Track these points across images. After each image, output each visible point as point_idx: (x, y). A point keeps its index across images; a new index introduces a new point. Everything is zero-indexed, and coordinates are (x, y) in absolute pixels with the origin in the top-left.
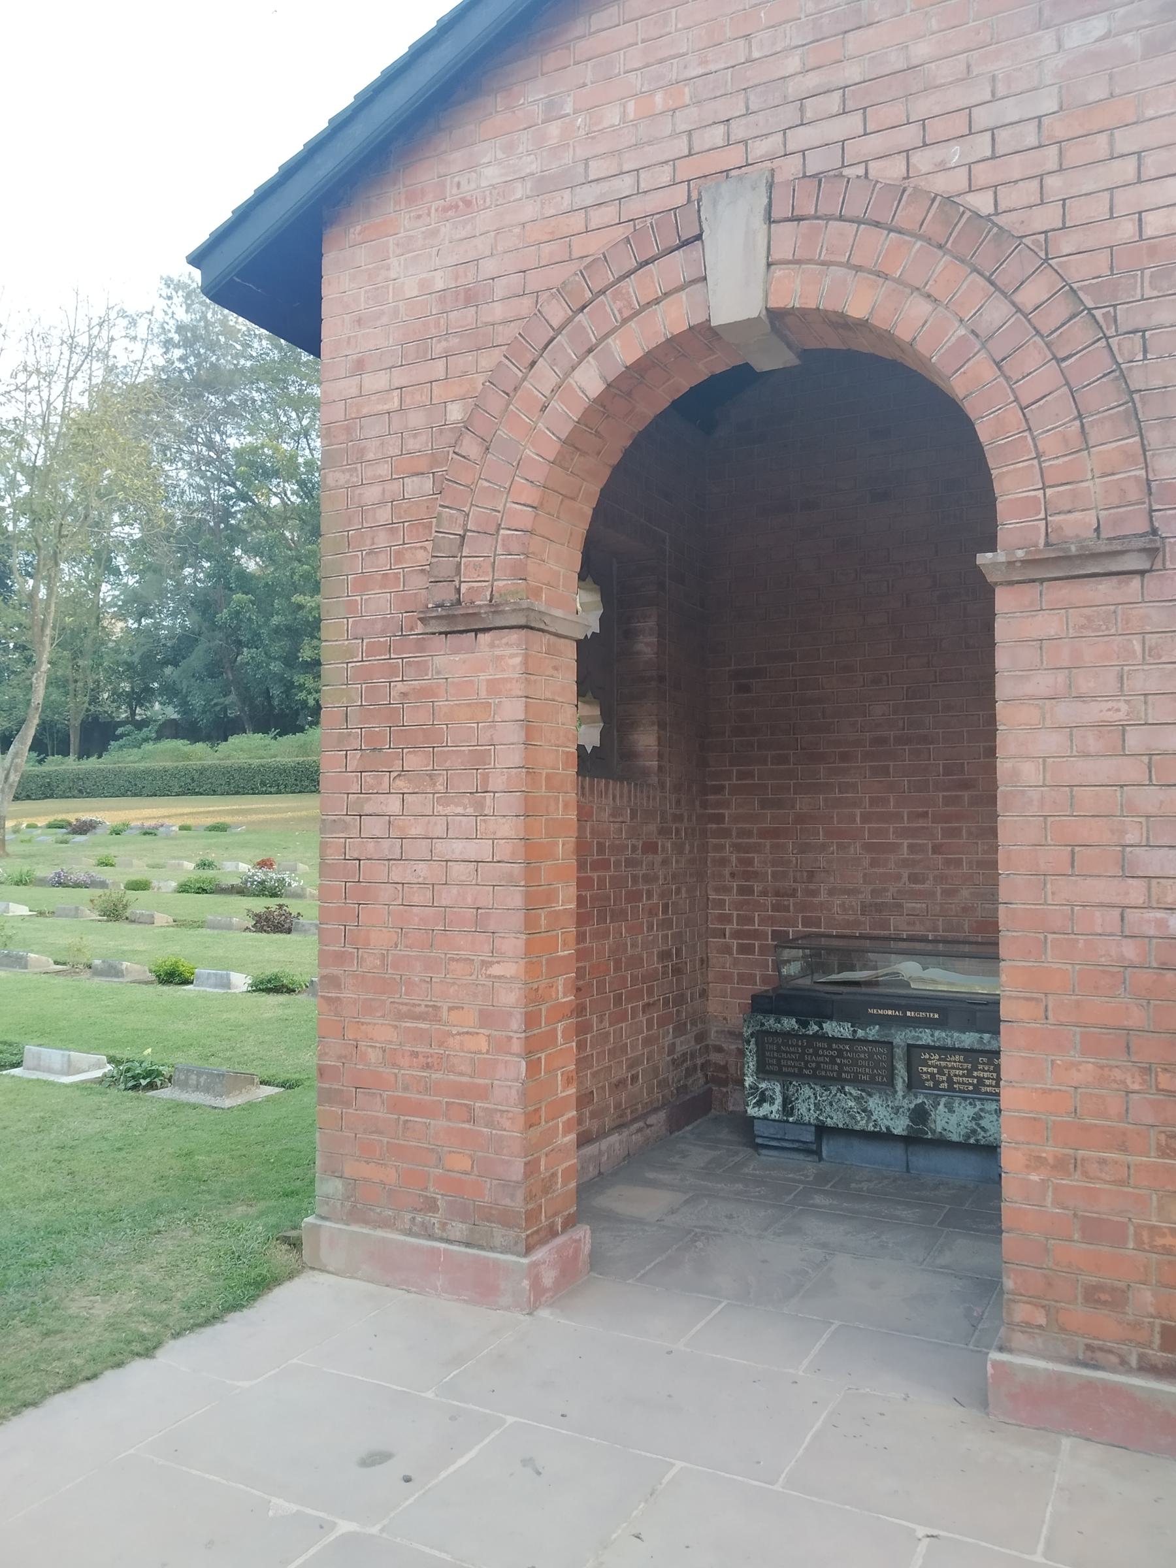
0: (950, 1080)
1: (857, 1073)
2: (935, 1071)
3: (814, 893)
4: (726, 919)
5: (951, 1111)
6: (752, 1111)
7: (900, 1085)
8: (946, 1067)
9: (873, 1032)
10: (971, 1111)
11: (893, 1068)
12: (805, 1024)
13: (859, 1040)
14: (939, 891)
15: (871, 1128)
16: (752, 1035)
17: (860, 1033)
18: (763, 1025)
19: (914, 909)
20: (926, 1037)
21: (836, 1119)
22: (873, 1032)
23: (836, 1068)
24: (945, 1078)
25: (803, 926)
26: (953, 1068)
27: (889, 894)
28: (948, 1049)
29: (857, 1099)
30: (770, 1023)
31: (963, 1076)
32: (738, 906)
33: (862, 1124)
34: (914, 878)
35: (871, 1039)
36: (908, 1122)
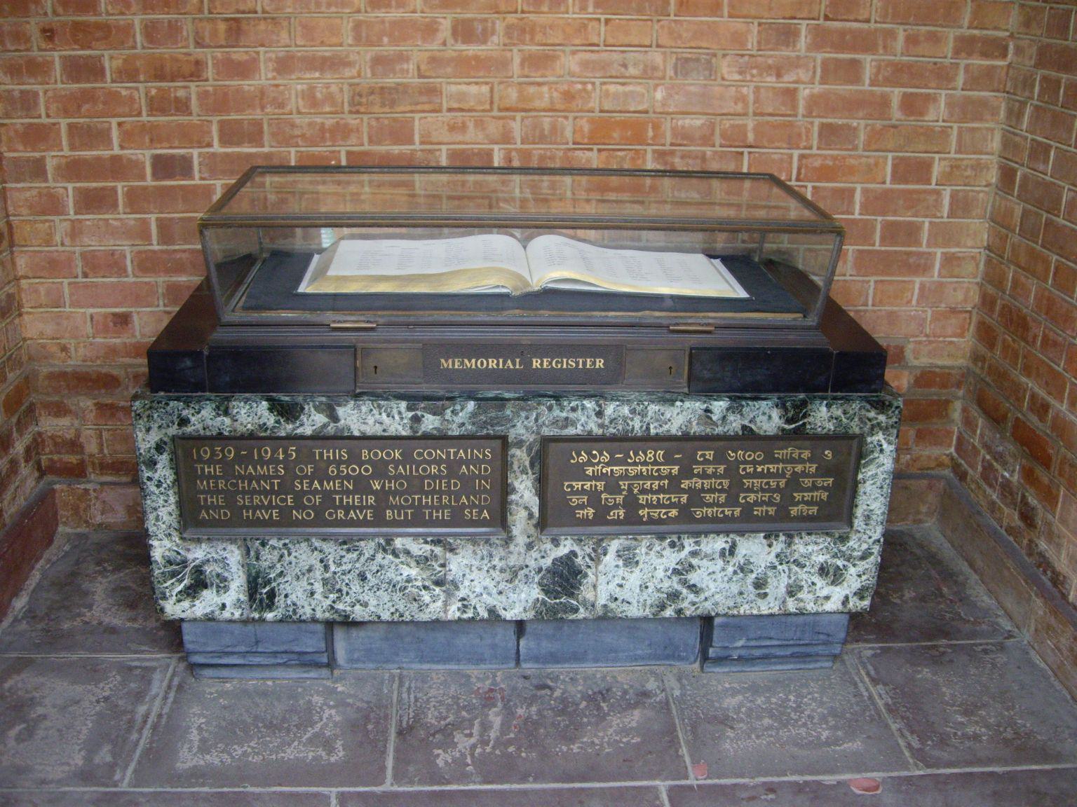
0: (631, 504)
1: (419, 509)
2: (600, 485)
3: (245, 69)
4: (38, 135)
5: (629, 560)
6: (173, 608)
7: (520, 523)
8: (625, 477)
9: (461, 417)
10: (671, 558)
11: (505, 490)
12: (289, 412)
13: (427, 437)
14: (517, 60)
15: (453, 612)
16: (159, 448)
17: (430, 423)
18: (184, 422)
19: (462, 97)
20: (584, 417)
21: (375, 604)
22: (461, 417)
23: (372, 500)
24: (620, 499)
25: (224, 141)
26: (639, 476)
27: (411, 67)
28: (636, 439)
29: (423, 561)
30: (204, 418)
31: (661, 490)
32: (70, 105)
33: (435, 606)
34: (464, 31)
35: (456, 432)
36: (536, 593)
